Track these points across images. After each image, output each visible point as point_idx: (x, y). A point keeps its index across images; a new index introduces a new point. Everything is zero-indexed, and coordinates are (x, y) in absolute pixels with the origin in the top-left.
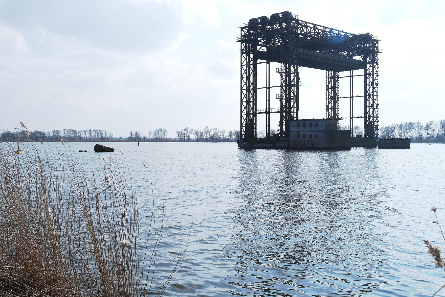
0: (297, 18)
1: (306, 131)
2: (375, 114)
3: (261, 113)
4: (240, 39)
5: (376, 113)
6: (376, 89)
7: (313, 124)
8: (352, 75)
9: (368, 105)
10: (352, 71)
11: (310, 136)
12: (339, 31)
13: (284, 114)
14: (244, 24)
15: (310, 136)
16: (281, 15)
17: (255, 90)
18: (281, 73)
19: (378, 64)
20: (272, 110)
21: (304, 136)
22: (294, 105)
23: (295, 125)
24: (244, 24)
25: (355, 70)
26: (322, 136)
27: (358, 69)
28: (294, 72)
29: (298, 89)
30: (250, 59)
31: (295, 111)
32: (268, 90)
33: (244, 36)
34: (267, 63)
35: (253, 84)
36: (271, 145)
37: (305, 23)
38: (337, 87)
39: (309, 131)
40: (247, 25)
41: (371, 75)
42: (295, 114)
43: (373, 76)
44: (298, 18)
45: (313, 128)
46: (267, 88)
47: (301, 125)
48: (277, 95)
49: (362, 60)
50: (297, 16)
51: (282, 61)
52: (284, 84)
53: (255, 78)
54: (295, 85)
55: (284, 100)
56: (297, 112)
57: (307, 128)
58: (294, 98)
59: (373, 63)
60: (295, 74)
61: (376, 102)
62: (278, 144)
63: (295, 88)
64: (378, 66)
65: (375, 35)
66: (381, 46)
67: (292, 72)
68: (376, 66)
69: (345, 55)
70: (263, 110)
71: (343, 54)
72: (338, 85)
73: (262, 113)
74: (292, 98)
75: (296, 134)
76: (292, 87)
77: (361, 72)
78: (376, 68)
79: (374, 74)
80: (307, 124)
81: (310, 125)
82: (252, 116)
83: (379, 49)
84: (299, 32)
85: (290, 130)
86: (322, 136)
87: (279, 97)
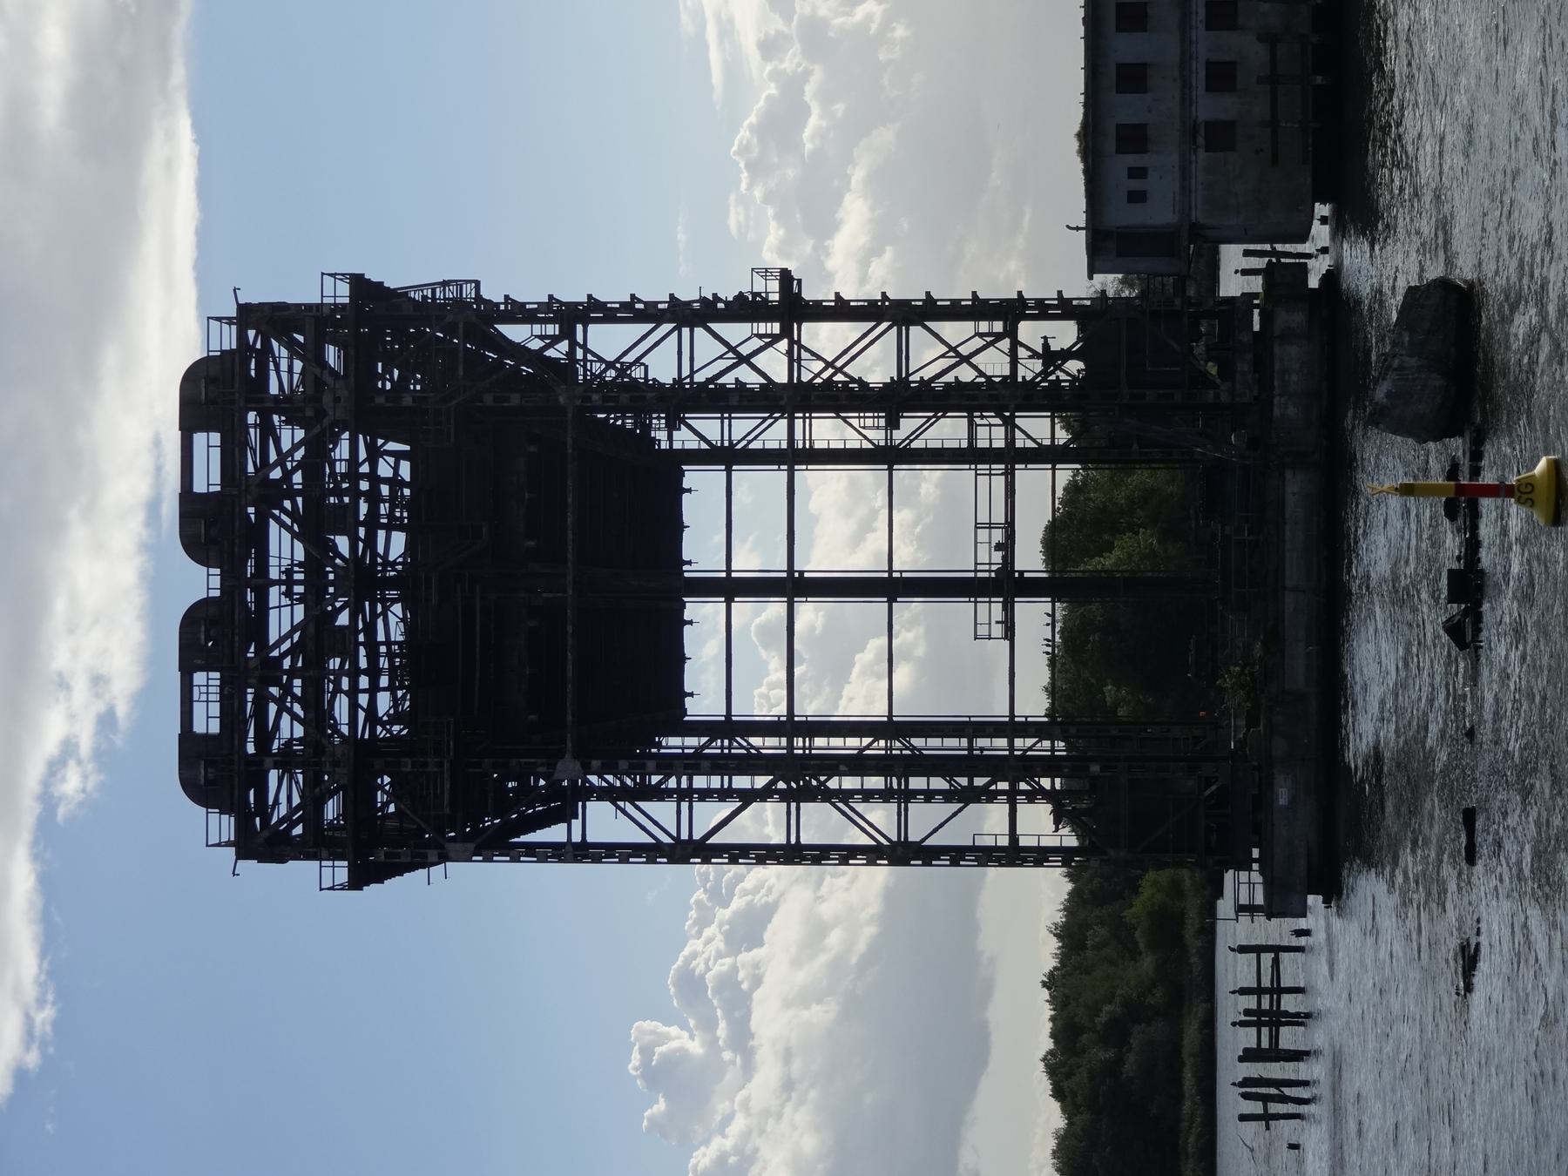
16: (199, 438)
21: (1221, 77)
25: (685, 557)
36: (1295, 487)
62: (1292, 411)
75: (1202, 154)
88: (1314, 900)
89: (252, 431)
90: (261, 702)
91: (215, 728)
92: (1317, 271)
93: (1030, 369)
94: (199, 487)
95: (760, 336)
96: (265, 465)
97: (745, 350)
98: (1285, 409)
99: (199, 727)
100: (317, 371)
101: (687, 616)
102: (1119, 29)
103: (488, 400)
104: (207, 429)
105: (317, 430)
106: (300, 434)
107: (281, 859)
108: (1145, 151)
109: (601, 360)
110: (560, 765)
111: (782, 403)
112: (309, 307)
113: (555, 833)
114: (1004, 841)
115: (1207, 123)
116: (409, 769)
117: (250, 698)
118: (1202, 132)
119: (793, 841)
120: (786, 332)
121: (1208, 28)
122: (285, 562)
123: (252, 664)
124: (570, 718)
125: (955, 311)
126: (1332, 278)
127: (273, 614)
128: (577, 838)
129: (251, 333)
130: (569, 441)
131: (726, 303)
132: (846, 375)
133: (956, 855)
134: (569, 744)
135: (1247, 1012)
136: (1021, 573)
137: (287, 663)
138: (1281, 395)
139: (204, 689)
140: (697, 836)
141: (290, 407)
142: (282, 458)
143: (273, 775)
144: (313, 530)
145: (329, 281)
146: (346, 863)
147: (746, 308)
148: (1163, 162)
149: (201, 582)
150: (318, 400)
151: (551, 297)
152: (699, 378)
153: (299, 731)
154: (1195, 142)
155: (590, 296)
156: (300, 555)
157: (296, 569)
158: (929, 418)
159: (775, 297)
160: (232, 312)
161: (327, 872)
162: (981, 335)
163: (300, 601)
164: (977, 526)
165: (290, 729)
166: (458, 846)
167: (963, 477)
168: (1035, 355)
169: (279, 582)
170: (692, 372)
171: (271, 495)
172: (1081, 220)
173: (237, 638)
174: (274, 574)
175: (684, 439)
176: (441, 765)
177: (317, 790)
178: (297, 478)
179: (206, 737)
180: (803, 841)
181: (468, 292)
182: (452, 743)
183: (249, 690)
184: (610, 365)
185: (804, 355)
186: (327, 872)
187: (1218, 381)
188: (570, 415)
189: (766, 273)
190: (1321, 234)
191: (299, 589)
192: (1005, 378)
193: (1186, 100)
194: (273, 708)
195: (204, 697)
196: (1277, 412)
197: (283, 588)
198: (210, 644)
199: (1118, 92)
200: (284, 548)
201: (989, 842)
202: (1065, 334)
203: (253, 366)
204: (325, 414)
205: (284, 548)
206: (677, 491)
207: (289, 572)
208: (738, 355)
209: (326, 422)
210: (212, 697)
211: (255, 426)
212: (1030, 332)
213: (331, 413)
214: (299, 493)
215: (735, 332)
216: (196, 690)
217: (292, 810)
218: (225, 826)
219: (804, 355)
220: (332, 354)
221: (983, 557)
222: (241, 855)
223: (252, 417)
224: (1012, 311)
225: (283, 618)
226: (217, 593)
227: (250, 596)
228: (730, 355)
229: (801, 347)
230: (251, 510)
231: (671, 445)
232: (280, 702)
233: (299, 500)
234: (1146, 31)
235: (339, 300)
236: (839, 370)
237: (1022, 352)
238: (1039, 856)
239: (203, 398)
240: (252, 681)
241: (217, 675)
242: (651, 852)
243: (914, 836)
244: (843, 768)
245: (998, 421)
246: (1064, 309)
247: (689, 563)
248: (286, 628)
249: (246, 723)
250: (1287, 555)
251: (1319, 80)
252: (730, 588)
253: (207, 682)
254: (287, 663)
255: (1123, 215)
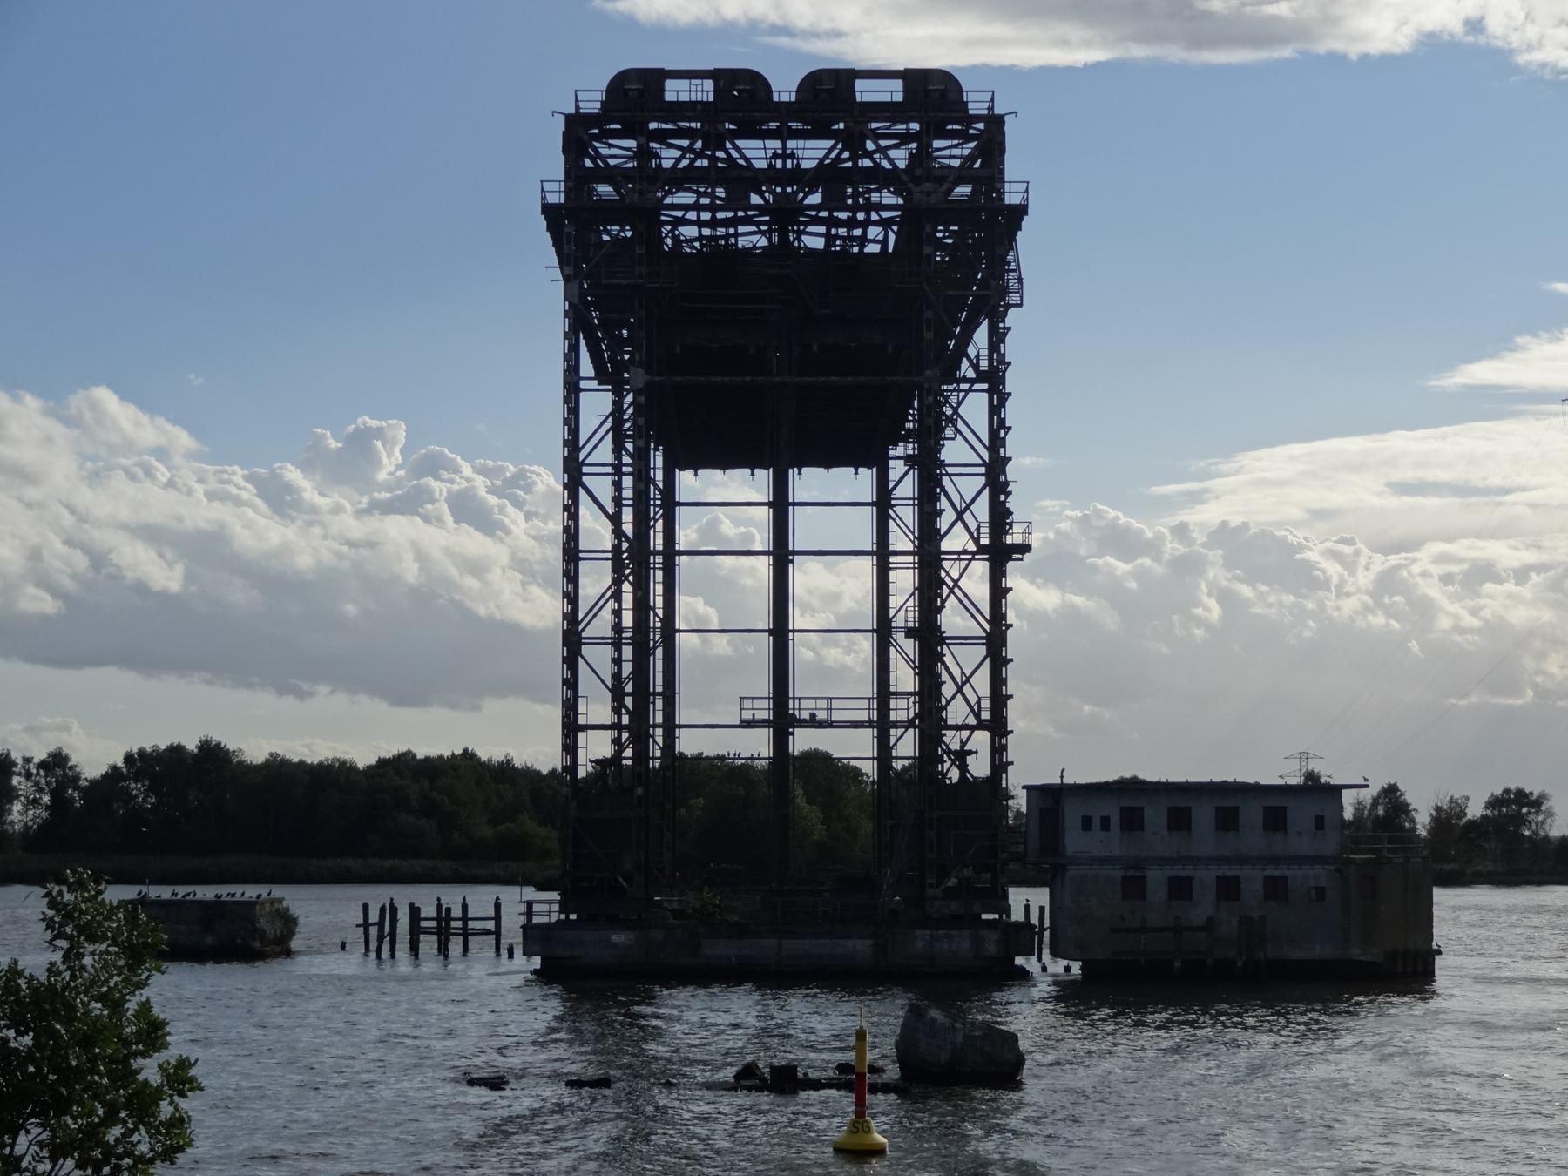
1: (1195, 861)
7: (1251, 814)
11: (1228, 889)
15: (1228, 889)
16: (898, 84)
21: (1180, 889)
26: (1313, 893)
36: (860, 947)
39: (1220, 860)
45: (1252, 838)
47: (1156, 817)
57: (1252, 838)
62: (919, 944)
75: (1120, 874)
80: (1204, 816)
81: (1227, 820)
86: (1321, 891)
88: (536, 962)
89: (904, 126)
90: (690, 134)
91: (669, 97)
92: (1030, 963)
93: (952, 740)
94: (860, 84)
95: (978, 529)
96: (877, 137)
97: (967, 516)
98: (921, 940)
99: (670, 84)
100: (951, 179)
101: (757, 471)
102: (1217, 808)
103: (929, 314)
104: (905, 91)
105: (905, 178)
106: (902, 165)
107: (565, 150)
108: (1121, 830)
109: (960, 403)
110: (641, 371)
111: (926, 546)
112: (1002, 172)
113: (587, 367)
114: (582, 720)
115: (1145, 877)
116: (638, 251)
117: (693, 125)
118: (1137, 874)
119: (581, 555)
120: (981, 549)
121: (1218, 877)
122: (800, 153)
123: (719, 127)
124: (678, 379)
125: (997, 681)
126: (1023, 976)
127: (758, 143)
128: (583, 384)
129: (981, 126)
130: (895, 378)
131: (1004, 502)
132: (948, 596)
133: (571, 683)
134: (657, 378)
135: (448, 910)
136: (793, 734)
137: (720, 154)
138: (931, 936)
139: (700, 88)
140: (585, 479)
141: (922, 157)
142: (882, 150)
143: (632, 144)
144: (826, 175)
145: (1023, 187)
146: (562, 201)
147: (1000, 517)
148: (1113, 843)
149: (784, 87)
150: (928, 180)
151: (1009, 363)
152: (946, 481)
153: (667, 164)
154: (1130, 868)
155: (1010, 394)
156: (806, 165)
157: (795, 162)
158: (914, 662)
159: (1009, 540)
160: (997, 111)
161: (555, 186)
162: (979, 702)
163: (770, 165)
164: (829, 699)
165: (668, 157)
166: (576, 290)
167: (869, 688)
168: (963, 744)
169: (784, 148)
170: (950, 475)
171: (853, 140)
172: (1069, 779)
173: (740, 115)
174: (791, 144)
175: (897, 468)
176: (640, 276)
177: (620, 179)
178: (867, 163)
179: (662, 90)
180: (581, 563)
181: (1013, 298)
182: (657, 285)
183: (699, 124)
184: (955, 410)
185: (964, 563)
186: (555, 186)
187: (943, 887)
188: (916, 379)
189: (1028, 532)
190: (1058, 967)
191: (779, 164)
192: (945, 721)
193: (1162, 861)
194: (685, 143)
195: (693, 88)
196: (918, 933)
197: (780, 152)
198: (735, 93)
199: (1169, 809)
200: (811, 152)
201: (581, 709)
202: (979, 767)
203: (956, 127)
204: (917, 185)
205: (811, 152)
206: (855, 460)
207: (792, 156)
208: (963, 512)
209: (911, 185)
210: (693, 94)
211: (908, 129)
212: (981, 739)
213: (918, 189)
214: (855, 164)
215: (982, 509)
216: (699, 81)
217: (604, 158)
218: (592, 105)
219: (964, 563)
220: (964, 190)
221: (804, 704)
222: (569, 118)
223: (915, 126)
224: (997, 726)
225: (757, 152)
226: (775, 98)
227: (773, 125)
228: (964, 505)
229: (970, 560)
230: (842, 126)
231: (892, 458)
232: (690, 149)
233: (849, 164)
234: (1217, 828)
235: (1007, 195)
236: (951, 591)
237: (965, 733)
238: (570, 748)
239: (931, 88)
240: (707, 127)
241: (711, 99)
242: (572, 443)
243: (586, 650)
244: (639, 594)
245: (912, 715)
246: (999, 767)
248: (748, 154)
249: (674, 122)
250: (807, 941)
251: (1178, 964)
252: (781, 505)
253: (705, 91)
254: (720, 154)
255: (1072, 813)
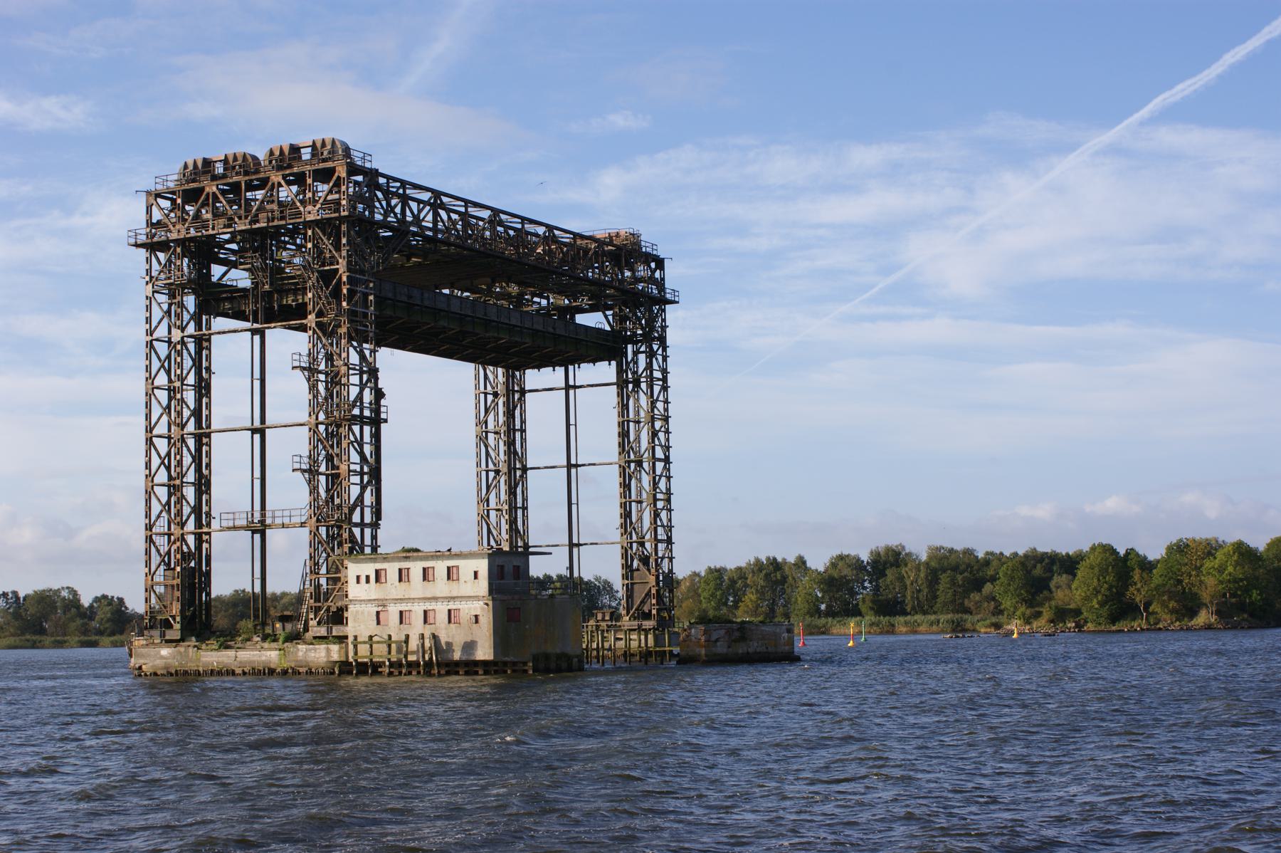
0: (368, 165)
1: (411, 600)
2: (660, 530)
3: (229, 529)
4: (142, 239)
5: (663, 526)
6: (661, 435)
8: (571, 383)
9: (633, 497)
10: (571, 368)
12: (524, 220)
13: (323, 531)
14: (158, 180)
17: (203, 438)
18: (311, 371)
19: (664, 347)
20: (274, 517)
22: (361, 497)
23: (368, 578)
24: (158, 180)
25: (582, 365)
27: (594, 361)
28: (361, 368)
29: (377, 437)
30: (186, 317)
31: (368, 519)
32: (257, 437)
33: (159, 224)
34: (254, 332)
35: (197, 413)
37: (398, 184)
38: (518, 427)
40: (171, 185)
41: (643, 386)
42: (368, 531)
43: (651, 387)
44: (375, 165)
46: (254, 431)
48: (297, 459)
49: (608, 328)
50: (369, 158)
51: (314, 325)
52: (322, 417)
53: (203, 388)
54: (367, 418)
55: (322, 479)
56: (375, 525)
58: (362, 468)
59: (648, 338)
60: (365, 377)
61: (662, 485)
62: (300, 654)
63: (367, 429)
64: (665, 349)
65: (651, 239)
66: (673, 276)
67: (354, 369)
68: (660, 352)
69: (543, 308)
70: (237, 516)
71: (539, 303)
72: (523, 422)
73: (235, 528)
74: (355, 471)
76: (354, 427)
77: (606, 371)
78: (660, 358)
79: (652, 380)
82: (191, 540)
83: (668, 291)
84: (378, 217)
85: (350, 597)
86: (476, 616)
87: (304, 467)
101: (556, 368)
110: (179, 331)
164: (290, 510)
247: (579, 367)
